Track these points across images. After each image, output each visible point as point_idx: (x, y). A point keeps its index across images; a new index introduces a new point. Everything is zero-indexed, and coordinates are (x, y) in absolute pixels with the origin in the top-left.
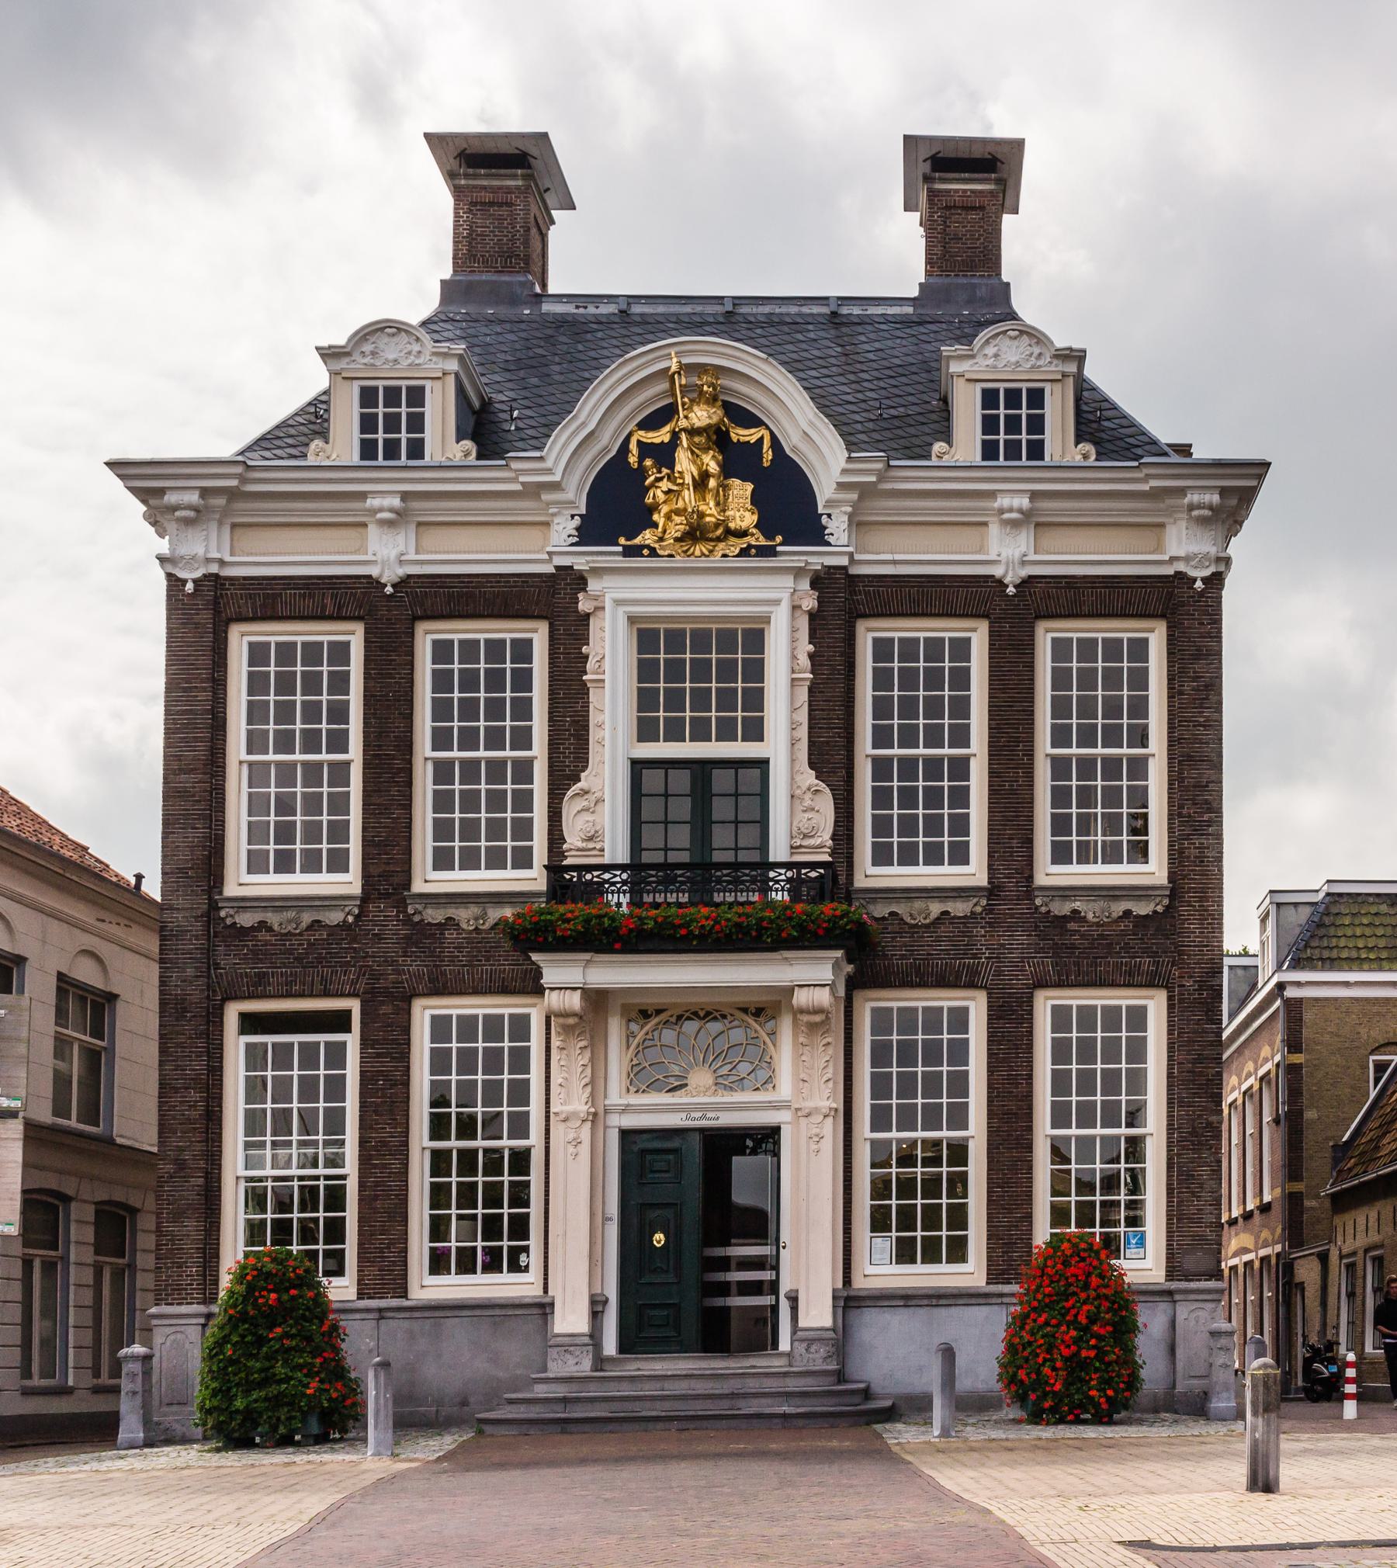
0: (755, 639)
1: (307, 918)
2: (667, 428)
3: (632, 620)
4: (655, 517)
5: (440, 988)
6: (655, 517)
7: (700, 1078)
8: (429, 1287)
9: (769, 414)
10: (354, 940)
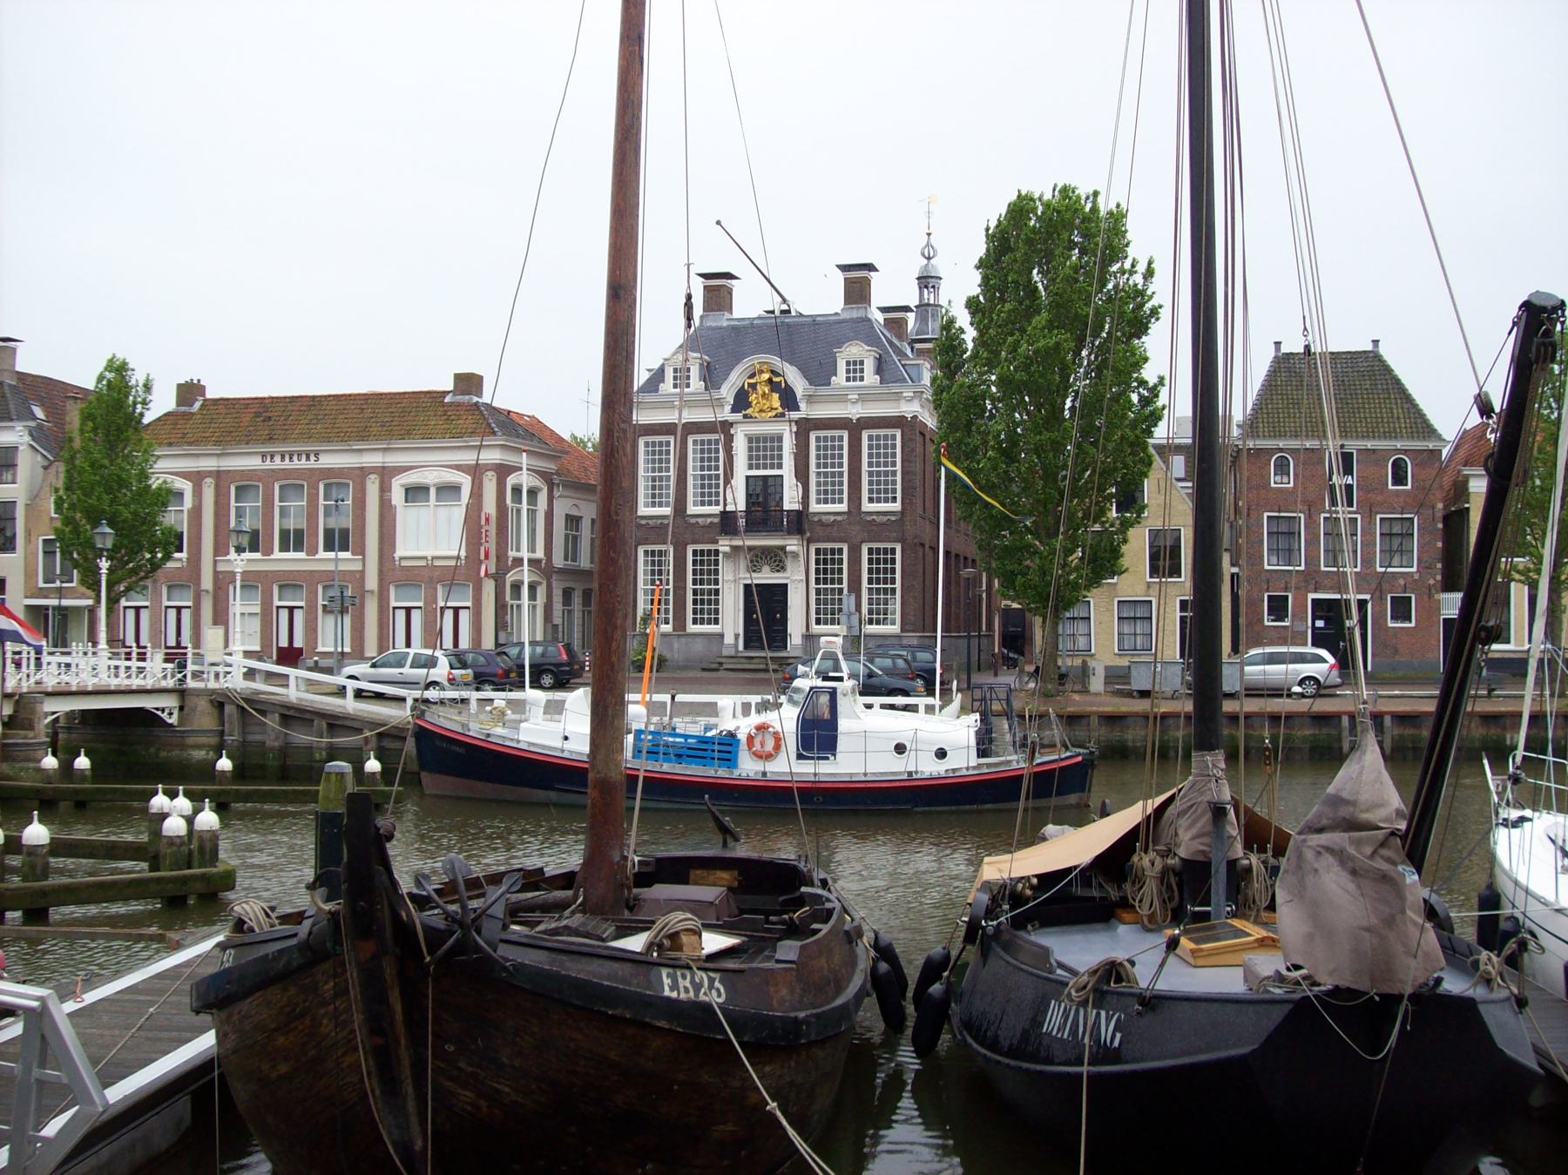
0: (780, 439)
5: (694, 542)
7: (766, 568)
8: (692, 628)
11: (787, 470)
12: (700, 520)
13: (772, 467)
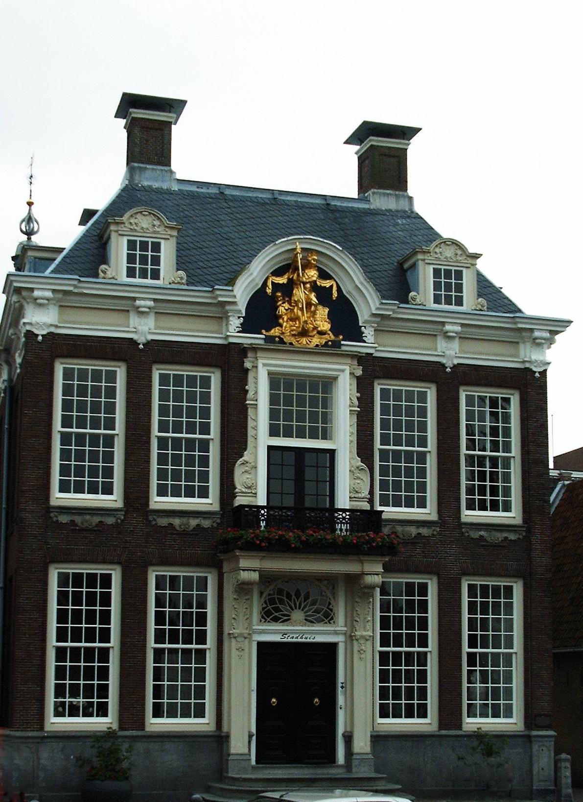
1: (96, 520)
2: (286, 276)
3: (269, 374)
4: (281, 321)
6: (281, 321)
8: (156, 724)
9: (334, 272)
10: (120, 533)
11: (343, 438)
12: (177, 522)
13: (314, 436)
